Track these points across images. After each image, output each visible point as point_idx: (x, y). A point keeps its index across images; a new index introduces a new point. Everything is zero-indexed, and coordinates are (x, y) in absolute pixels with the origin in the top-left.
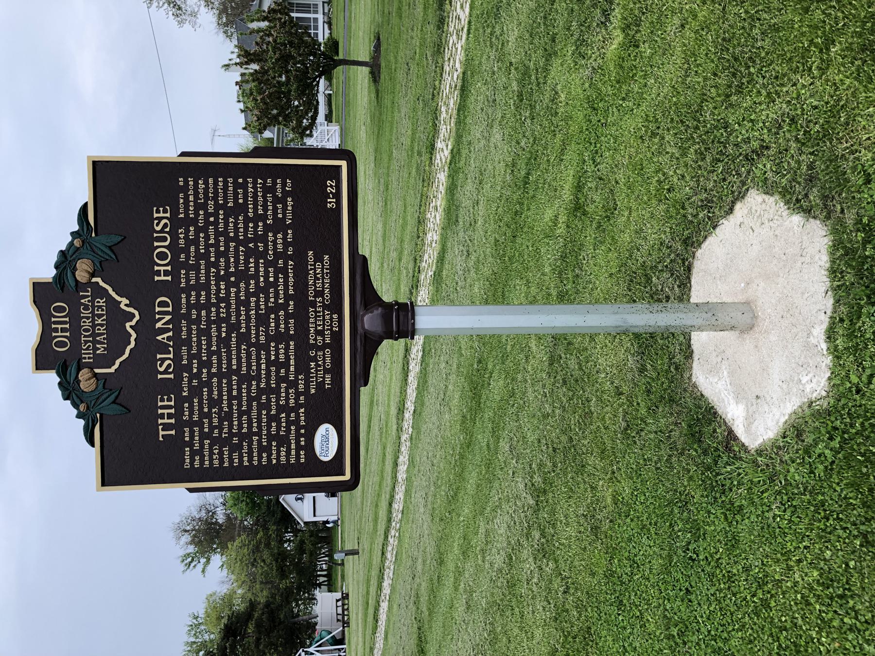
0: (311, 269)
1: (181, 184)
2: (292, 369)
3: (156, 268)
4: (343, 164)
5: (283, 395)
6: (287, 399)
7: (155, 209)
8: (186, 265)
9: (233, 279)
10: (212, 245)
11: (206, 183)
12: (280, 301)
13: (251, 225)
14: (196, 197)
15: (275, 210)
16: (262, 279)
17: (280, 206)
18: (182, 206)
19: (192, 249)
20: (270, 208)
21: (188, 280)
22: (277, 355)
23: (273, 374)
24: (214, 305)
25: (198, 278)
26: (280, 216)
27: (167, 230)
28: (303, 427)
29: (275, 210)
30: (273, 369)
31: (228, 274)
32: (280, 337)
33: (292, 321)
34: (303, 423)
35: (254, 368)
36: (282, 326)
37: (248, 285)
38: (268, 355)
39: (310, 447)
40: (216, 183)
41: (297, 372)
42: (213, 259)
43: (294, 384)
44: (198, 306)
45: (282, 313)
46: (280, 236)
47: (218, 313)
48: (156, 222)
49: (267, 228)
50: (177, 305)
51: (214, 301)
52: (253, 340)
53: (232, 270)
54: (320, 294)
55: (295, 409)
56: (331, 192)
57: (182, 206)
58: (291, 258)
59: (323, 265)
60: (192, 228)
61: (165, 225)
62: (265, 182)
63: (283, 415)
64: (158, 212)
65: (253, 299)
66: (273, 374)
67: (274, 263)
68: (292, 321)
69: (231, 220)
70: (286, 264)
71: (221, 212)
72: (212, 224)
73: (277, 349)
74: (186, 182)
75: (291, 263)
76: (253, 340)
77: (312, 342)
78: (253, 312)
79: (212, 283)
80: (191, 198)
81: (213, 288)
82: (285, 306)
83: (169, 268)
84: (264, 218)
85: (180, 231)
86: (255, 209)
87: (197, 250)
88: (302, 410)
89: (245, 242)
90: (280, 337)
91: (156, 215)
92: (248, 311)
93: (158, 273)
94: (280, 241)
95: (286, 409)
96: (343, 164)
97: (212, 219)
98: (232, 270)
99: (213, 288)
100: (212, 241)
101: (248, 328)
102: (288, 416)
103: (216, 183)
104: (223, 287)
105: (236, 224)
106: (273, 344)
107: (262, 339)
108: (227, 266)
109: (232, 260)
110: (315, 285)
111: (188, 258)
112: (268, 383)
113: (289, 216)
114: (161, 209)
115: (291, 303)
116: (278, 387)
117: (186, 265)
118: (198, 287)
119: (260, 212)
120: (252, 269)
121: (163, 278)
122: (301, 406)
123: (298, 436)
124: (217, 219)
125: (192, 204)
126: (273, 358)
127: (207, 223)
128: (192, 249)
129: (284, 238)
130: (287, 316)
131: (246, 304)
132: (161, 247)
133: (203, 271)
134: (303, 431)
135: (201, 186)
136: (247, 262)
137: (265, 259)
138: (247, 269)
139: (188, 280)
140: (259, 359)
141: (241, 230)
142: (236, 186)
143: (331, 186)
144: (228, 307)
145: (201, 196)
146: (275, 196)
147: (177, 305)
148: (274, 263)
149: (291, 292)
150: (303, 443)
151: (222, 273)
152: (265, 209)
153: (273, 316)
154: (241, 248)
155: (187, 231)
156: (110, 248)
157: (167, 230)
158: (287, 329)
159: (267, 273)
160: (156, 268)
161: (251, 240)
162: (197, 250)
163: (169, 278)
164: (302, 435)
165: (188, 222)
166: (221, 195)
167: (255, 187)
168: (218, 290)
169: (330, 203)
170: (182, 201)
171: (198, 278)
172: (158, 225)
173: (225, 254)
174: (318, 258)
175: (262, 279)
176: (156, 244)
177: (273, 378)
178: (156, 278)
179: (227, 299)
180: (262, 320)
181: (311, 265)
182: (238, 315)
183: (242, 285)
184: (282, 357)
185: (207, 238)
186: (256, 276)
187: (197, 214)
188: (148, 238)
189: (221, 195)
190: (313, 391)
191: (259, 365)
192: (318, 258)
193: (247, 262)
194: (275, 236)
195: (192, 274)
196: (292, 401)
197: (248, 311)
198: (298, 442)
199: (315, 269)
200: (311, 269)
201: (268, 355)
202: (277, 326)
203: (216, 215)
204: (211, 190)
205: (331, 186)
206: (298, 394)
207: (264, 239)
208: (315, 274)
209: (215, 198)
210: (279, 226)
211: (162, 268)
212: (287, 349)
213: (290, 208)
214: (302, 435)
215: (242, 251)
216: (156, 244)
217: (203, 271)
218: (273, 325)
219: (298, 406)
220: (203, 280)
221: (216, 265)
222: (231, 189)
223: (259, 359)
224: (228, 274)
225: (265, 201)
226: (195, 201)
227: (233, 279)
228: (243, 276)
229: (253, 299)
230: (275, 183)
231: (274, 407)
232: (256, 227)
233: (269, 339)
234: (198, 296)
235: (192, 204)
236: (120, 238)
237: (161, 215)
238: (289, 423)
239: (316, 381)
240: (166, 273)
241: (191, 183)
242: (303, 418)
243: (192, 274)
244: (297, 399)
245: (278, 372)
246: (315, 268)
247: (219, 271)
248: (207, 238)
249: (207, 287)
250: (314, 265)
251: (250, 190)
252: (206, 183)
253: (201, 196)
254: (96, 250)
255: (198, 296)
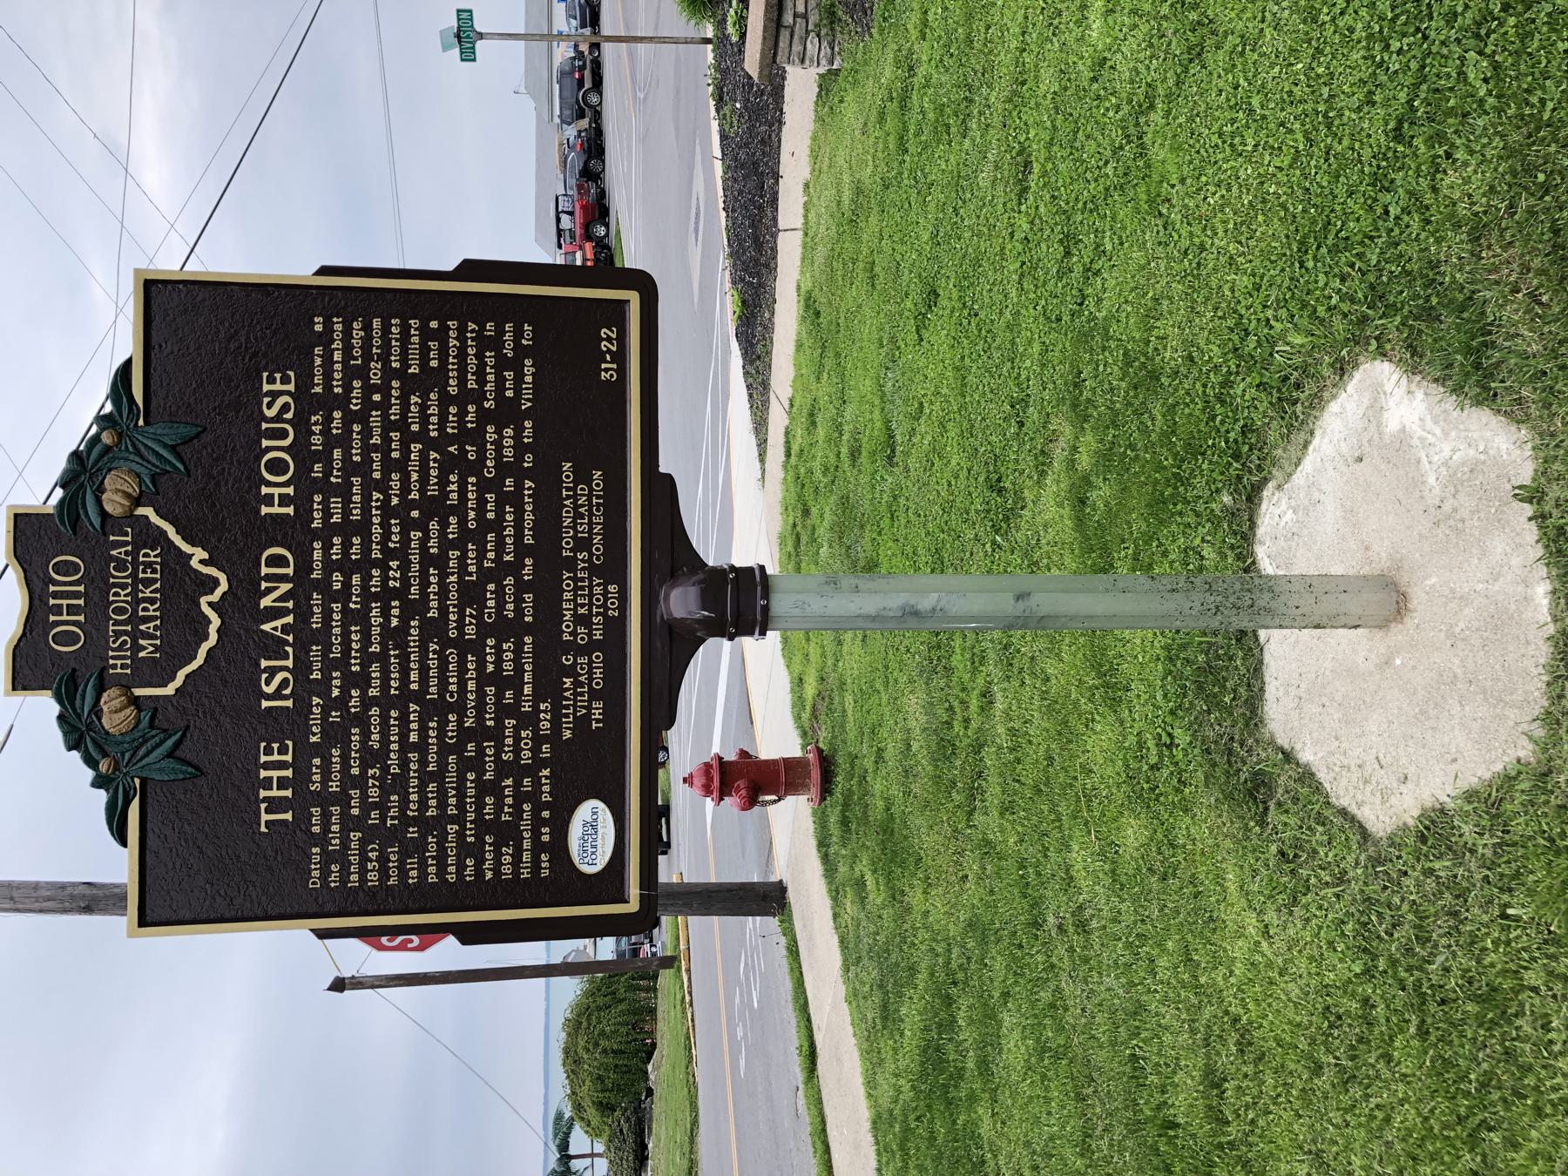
0: (568, 497)
1: (318, 328)
2: (527, 690)
3: (265, 490)
4: (633, 297)
5: (509, 741)
6: (517, 751)
7: (265, 374)
8: (324, 487)
9: (415, 514)
10: (376, 448)
11: (367, 327)
12: (507, 558)
13: (453, 410)
14: (347, 350)
15: (500, 381)
16: (472, 514)
17: (509, 375)
18: (318, 371)
19: (337, 454)
20: (491, 378)
21: (327, 514)
22: (499, 662)
23: (490, 700)
24: (376, 563)
25: (346, 512)
26: (510, 394)
27: (289, 416)
28: (547, 806)
29: (500, 381)
30: (491, 690)
31: (407, 505)
32: (506, 629)
33: (528, 597)
34: (546, 798)
35: (453, 688)
36: (510, 606)
37: (444, 525)
38: (481, 664)
39: (559, 846)
40: (386, 329)
41: (537, 697)
42: (377, 475)
43: (531, 720)
44: (347, 567)
45: (509, 580)
46: (509, 432)
47: (385, 579)
48: (266, 400)
49: (484, 417)
50: (304, 566)
51: (376, 554)
52: (453, 634)
53: (414, 495)
54: (583, 544)
55: (532, 770)
56: (609, 351)
57: (318, 371)
58: (528, 473)
59: (591, 490)
60: (337, 415)
61: (285, 408)
62: (482, 328)
63: (509, 782)
64: (271, 381)
65: (454, 554)
66: (490, 700)
67: (495, 485)
68: (528, 597)
69: (414, 399)
70: (519, 486)
71: (395, 384)
72: (376, 406)
73: (499, 652)
74: (328, 325)
75: (528, 484)
76: (453, 634)
77: (566, 637)
78: (453, 578)
79: (375, 520)
80: (337, 356)
81: (377, 530)
82: (516, 568)
83: (290, 490)
84: (480, 396)
85: (314, 419)
86: (462, 380)
87: (347, 456)
88: (546, 772)
89: (439, 444)
90: (506, 629)
91: (266, 388)
92: (443, 575)
93: (269, 500)
94: (507, 442)
95: (514, 769)
96: (633, 297)
97: (377, 397)
98: (414, 495)
99: (377, 530)
100: (376, 440)
101: (443, 611)
102: (518, 784)
103: (386, 329)
104: (396, 530)
105: (423, 408)
106: (490, 642)
107: (471, 631)
108: (405, 489)
109: (415, 476)
110: (574, 528)
111: (327, 473)
112: (480, 718)
113: (527, 394)
114: (278, 376)
115: (528, 561)
116: (500, 726)
117: (324, 487)
118: (347, 529)
119: (472, 385)
120: (454, 496)
121: (276, 510)
122: (544, 763)
123: (537, 823)
124: (387, 396)
125: (338, 367)
126: (490, 668)
127: (368, 405)
128: (337, 454)
129: (517, 437)
130: (521, 587)
131: (441, 562)
132: (276, 449)
133: (356, 498)
134: (546, 814)
135: (358, 333)
136: (443, 482)
137: (479, 475)
138: (445, 495)
139: (327, 514)
140: (462, 669)
141: (434, 419)
142: (426, 334)
143: (609, 339)
144: (405, 567)
145: (357, 352)
146: (500, 357)
147: (304, 566)
148: (495, 485)
149: (528, 540)
150: (545, 838)
151: (395, 501)
152: (482, 381)
153: (491, 587)
154: (433, 455)
155: (329, 419)
156: (173, 449)
157: (289, 416)
158: (519, 611)
159: (482, 502)
160: (265, 490)
161: (452, 439)
162: (347, 456)
163: (290, 510)
164: (545, 822)
165: (328, 403)
166: (396, 350)
167: (461, 338)
168: (386, 535)
169: (606, 370)
170: (318, 361)
171: (346, 512)
172: (269, 406)
173: (402, 466)
174: (582, 477)
175: (472, 514)
176: (265, 443)
177: (490, 708)
178: (265, 510)
179: (402, 554)
180: (471, 595)
181: (568, 489)
182: (424, 584)
183: (434, 526)
184: (508, 666)
185: (367, 433)
186: (460, 510)
187: (348, 388)
188: (252, 428)
189: (396, 350)
190: (567, 734)
191: (462, 684)
192: (582, 477)
193: (443, 482)
194: (499, 432)
195: (336, 504)
196: (526, 754)
197: (443, 575)
198: (536, 835)
199: (575, 497)
200: (568, 497)
201: (481, 664)
202: (501, 605)
203: (385, 390)
204: (376, 342)
205: (609, 339)
206: (538, 740)
207: (477, 437)
208: (576, 507)
209: (385, 359)
210: (507, 413)
211: (276, 491)
212: (518, 651)
213: (529, 379)
214: (545, 822)
215: (435, 460)
216: (265, 443)
217: (356, 498)
218: (491, 603)
219: (539, 763)
220: (356, 514)
221: (383, 485)
222: (415, 339)
223: (462, 669)
224: (407, 505)
225: (482, 365)
226: (345, 362)
227: (415, 514)
228: (435, 508)
229: (454, 554)
230: (500, 332)
231: (490, 766)
232: (462, 413)
233: (484, 630)
234: (346, 546)
235: (338, 367)
236: (195, 431)
237: (278, 387)
238: (519, 798)
239: (575, 711)
240: (284, 500)
241: (338, 327)
242: (546, 788)
243: (336, 504)
244: (536, 750)
245: (499, 696)
246: (576, 494)
247: (388, 498)
248: (367, 433)
249: (364, 528)
250: (574, 489)
251: (453, 342)
252: (367, 327)
253: (357, 352)
254: (142, 449)
255: (346, 546)
